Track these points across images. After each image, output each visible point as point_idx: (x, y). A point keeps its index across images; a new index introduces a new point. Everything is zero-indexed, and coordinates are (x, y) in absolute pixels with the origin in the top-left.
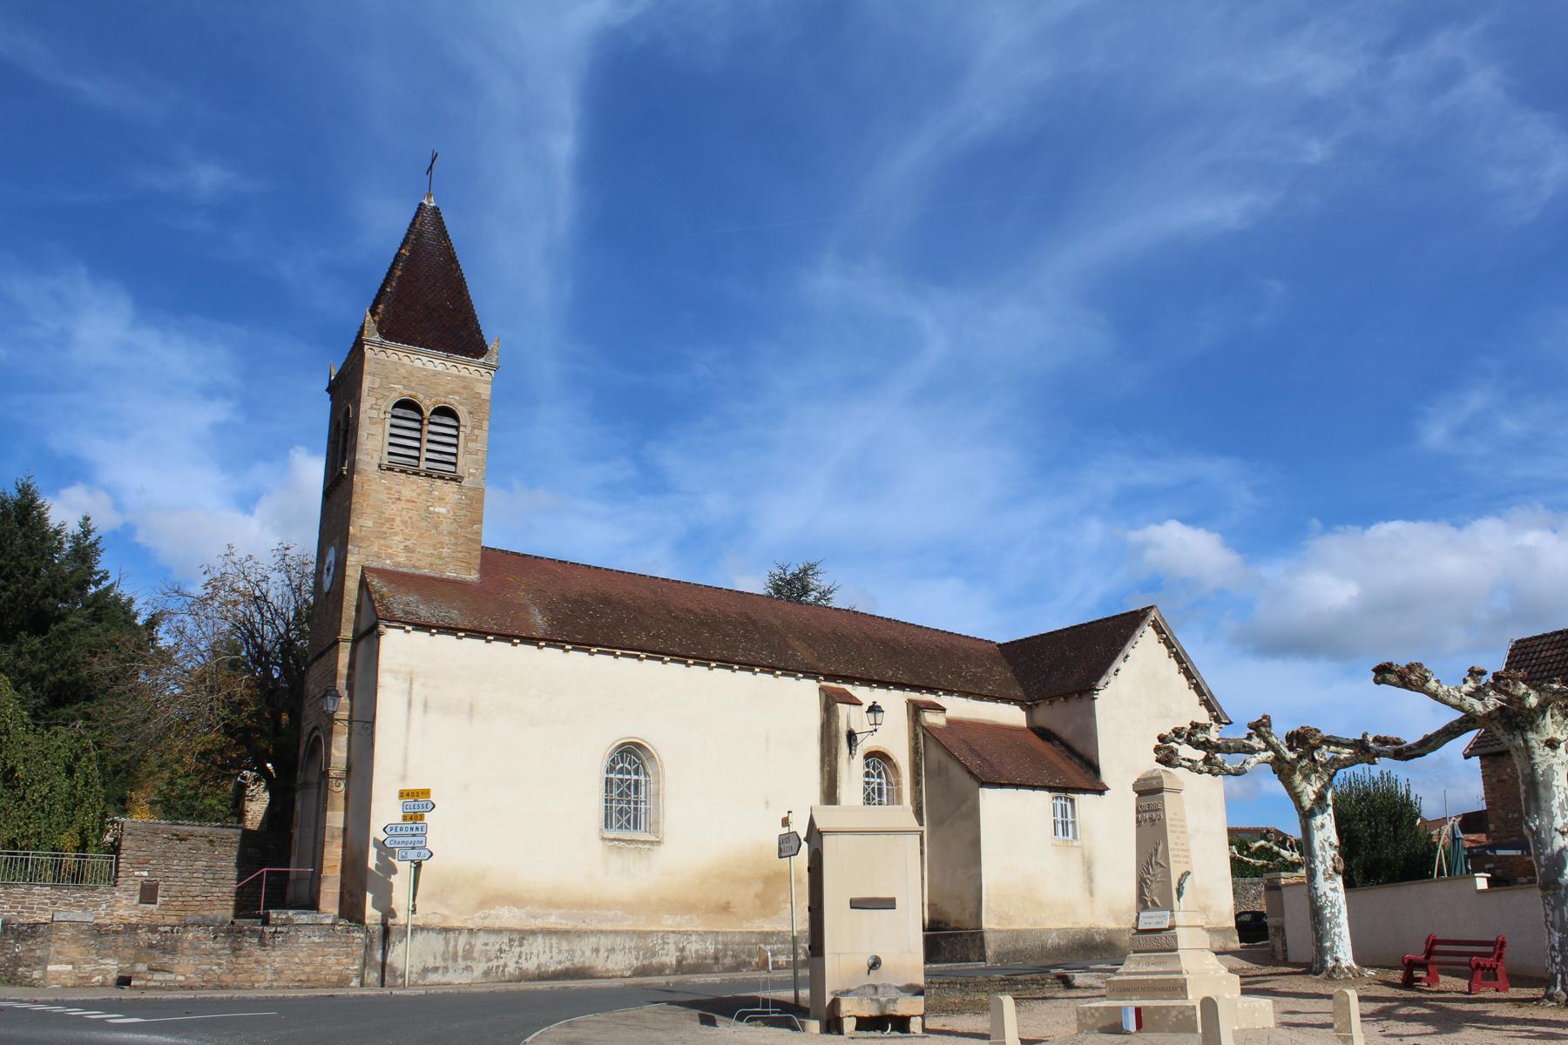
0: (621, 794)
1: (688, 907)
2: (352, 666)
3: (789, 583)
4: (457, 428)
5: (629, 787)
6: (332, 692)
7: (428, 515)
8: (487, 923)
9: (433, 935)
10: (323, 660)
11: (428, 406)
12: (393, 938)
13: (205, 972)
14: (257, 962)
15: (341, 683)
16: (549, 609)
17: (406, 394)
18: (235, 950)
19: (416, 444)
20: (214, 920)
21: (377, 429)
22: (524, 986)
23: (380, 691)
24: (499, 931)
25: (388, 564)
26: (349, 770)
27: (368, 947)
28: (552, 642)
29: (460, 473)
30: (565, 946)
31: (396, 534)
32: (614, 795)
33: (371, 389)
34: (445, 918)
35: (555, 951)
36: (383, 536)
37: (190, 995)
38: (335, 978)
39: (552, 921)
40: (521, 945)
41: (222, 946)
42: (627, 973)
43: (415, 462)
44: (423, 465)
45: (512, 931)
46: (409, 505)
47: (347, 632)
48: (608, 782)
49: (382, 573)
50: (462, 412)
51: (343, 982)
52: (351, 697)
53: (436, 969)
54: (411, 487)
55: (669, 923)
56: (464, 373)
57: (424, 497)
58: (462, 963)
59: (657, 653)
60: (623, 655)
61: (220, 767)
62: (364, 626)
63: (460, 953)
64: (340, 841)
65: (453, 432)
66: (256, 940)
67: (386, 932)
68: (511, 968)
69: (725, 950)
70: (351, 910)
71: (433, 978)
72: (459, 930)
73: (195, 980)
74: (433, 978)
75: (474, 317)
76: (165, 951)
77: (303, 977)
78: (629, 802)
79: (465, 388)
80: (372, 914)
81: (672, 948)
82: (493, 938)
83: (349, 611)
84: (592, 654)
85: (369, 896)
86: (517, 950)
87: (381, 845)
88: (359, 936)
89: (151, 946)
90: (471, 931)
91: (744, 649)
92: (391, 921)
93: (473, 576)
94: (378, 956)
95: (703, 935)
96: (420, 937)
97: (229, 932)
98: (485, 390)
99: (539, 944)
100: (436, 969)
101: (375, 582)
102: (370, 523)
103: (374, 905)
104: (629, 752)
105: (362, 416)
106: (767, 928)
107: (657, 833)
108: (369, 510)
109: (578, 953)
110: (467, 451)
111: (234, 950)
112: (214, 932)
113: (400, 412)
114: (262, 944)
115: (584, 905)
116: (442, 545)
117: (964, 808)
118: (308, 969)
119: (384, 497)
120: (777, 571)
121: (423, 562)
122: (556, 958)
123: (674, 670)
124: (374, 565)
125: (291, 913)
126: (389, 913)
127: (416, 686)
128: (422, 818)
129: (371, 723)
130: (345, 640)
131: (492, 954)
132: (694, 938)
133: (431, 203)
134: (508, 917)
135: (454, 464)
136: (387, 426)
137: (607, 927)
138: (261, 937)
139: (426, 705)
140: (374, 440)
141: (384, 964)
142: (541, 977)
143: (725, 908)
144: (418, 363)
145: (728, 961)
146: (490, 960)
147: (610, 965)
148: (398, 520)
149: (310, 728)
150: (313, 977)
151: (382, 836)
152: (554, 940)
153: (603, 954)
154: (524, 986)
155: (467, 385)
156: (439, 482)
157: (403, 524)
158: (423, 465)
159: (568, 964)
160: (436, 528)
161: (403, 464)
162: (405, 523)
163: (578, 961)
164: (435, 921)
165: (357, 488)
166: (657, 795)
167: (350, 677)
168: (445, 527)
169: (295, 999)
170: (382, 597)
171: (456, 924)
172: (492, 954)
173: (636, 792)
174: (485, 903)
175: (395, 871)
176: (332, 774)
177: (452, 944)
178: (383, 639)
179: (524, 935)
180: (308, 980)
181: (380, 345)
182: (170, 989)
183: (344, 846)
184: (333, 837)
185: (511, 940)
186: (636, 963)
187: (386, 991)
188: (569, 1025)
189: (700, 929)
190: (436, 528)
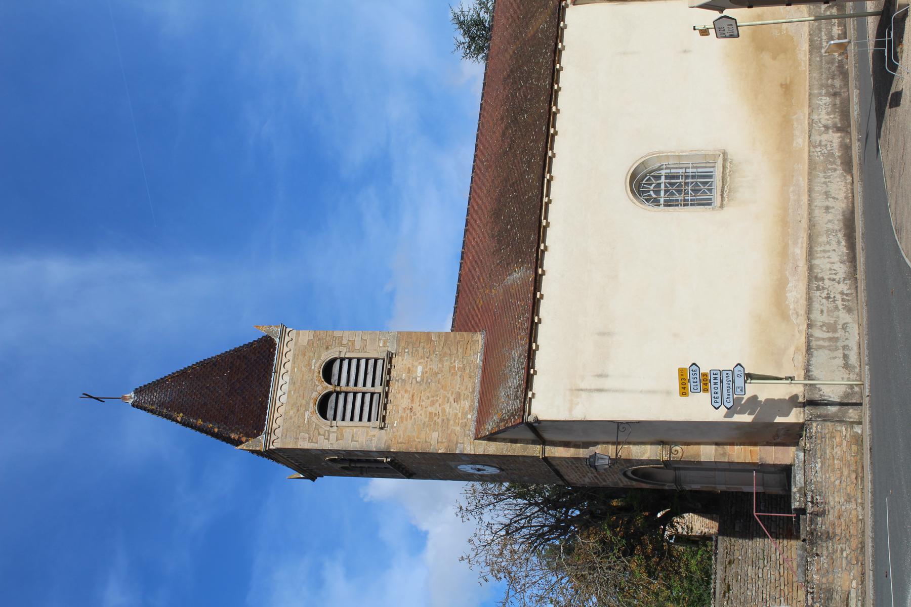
0: (679, 192)
1: (786, 124)
2: (566, 444)
3: (472, 38)
4: (342, 360)
5: (672, 184)
6: (591, 462)
8: (802, 311)
9: (814, 361)
10: (563, 470)
11: (324, 387)
12: (817, 397)
13: (849, 563)
14: (839, 518)
15: (583, 453)
16: (507, 266)
17: (313, 408)
18: (829, 537)
19: (359, 396)
20: (802, 557)
21: (347, 433)
22: (861, 275)
23: (589, 418)
24: (810, 300)
25: (471, 417)
26: (662, 443)
27: (825, 419)
28: (538, 262)
29: (384, 355)
30: (823, 239)
31: (444, 410)
32: (680, 197)
33: (310, 440)
34: (798, 349)
35: (828, 248)
36: (445, 422)
37: (870, 574)
38: (854, 448)
39: (799, 251)
40: (822, 279)
41: (825, 549)
42: (849, 179)
43: (376, 397)
44: (378, 389)
45: (809, 288)
46: (417, 400)
47: (535, 450)
48: (668, 204)
49: (480, 422)
50: (326, 356)
51: (858, 440)
52: (595, 444)
53: (845, 357)
54: (399, 399)
55: (801, 141)
56: (290, 356)
57: (408, 387)
58: (840, 334)
59: (545, 164)
60: (548, 195)
61: (662, 559)
62: (531, 435)
63: (830, 335)
64: (728, 448)
65: (346, 363)
66: (820, 519)
67: (811, 403)
68: (844, 287)
69: (827, 86)
70: (791, 435)
71: (853, 359)
72: (809, 336)
73: (856, 571)
74: (853, 359)
75: (237, 350)
76: (829, 599)
77: (853, 476)
78: (687, 184)
79: (305, 355)
80: (795, 417)
81: (824, 137)
82: (816, 306)
83: (517, 449)
84: (548, 224)
85: (778, 420)
86: (827, 282)
87: (731, 411)
88: (814, 427)
90: (809, 326)
91: (538, 80)
92: (801, 400)
93: (480, 338)
94: (833, 409)
95: (812, 109)
96: (815, 372)
97: (812, 543)
98: (305, 336)
99: (822, 264)
100: (845, 357)
101: (489, 427)
102: (435, 435)
103: (787, 415)
104: (639, 185)
105: (335, 447)
106: (805, 46)
107: (715, 156)
108: (423, 436)
109: (830, 226)
110: (364, 349)
111: (829, 538)
112: (812, 556)
113: (330, 413)
114: (823, 513)
115: (784, 221)
116: (452, 368)
118: (845, 473)
119: (409, 423)
120: (461, 51)
121: (469, 385)
122: (834, 246)
123: (560, 145)
124: (473, 429)
125: (794, 489)
126: (793, 401)
127: (583, 386)
128: (705, 375)
129: (620, 426)
130: (544, 451)
131: (831, 306)
132: (815, 117)
133: (131, 396)
134: (796, 292)
135: (376, 360)
136: (344, 423)
137: (805, 199)
138: (816, 515)
139: (600, 376)
140: (357, 435)
141: (841, 404)
142: (852, 259)
143: (787, 88)
144: (284, 399)
145: (838, 83)
146: (837, 308)
147: (841, 195)
148: (430, 409)
149: (625, 480)
150: (853, 467)
151: (723, 410)
152: (818, 249)
153: (830, 203)
154: (861, 275)
155: (302, 352)
156: (393, 373)
157: (434, 405)
158: (378, 389)
159: (840, 235)
160: (436, 374)
161: (378, 408)
162: (433, 403)
163: (838, 225)
164: (800, 359)
165: (403, 448)
166: (679, 157)
167: (577, 446)
168: (435, 367)
169: (873, 482)
170: (502, 420)
171: (803, 339)
172: (831, 306)
173: (677, 177)
174: (784, 315)
175: (754, 398)
176: (666, 458)
177: (821, 343)
178: (540, 418)
179: (813, 277)
180: (856, 471)
181: (267, 434)
182: (864, 592)
183: (732, 444)
184: (724, 454)
185: (818, 289)
186: (840, 171)
187: (866, 401)
188: (899, 231)
189: (806, 111)
190: (436, 374)
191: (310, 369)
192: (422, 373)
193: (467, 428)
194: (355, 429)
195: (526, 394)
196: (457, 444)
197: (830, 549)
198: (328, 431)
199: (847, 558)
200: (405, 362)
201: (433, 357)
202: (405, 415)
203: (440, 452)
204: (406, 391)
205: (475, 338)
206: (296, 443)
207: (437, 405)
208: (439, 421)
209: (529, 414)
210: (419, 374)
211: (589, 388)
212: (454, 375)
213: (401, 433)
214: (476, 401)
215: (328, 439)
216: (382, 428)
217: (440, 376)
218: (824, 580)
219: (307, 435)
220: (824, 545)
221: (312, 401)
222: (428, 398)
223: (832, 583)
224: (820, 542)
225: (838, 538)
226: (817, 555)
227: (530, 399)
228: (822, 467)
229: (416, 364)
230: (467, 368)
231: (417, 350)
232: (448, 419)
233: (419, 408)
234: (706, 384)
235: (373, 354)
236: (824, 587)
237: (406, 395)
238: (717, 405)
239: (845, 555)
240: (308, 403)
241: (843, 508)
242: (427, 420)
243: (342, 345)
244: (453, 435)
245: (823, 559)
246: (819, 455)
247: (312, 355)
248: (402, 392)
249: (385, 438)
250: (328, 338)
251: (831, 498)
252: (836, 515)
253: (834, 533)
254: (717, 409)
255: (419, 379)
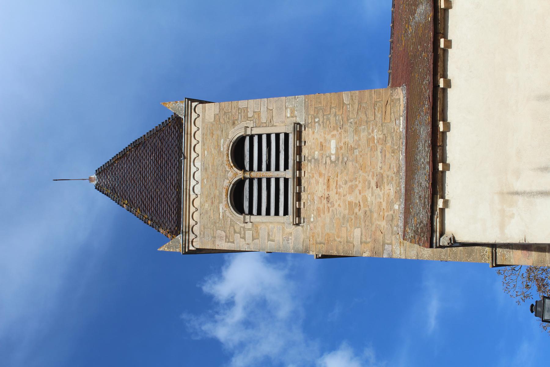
4: (252, 137)
7: (341, 161)
21: (263, 231)
25: (398, 207)
31: (365, 199)
33: (227, 239)
36: (368, 215)
46: (333, 185)
50: (235, 133)
57: (322, 169)
110: (270, 123)
116: (370, 140)
119: (327, 217)
127: (518, 186)
148: (350, 198)
158: (289, 174)
160: (352, 149)
162: (352, 189)
168: (350, 139)
190: (352, 149)
191: (219, 152)
192: (337, 149)
193: (395, 222)
194: (271, 226)
195: (433, 204)
196: (384, 245)
198: (244, 228)
200: (316, 136)
201: (347, 126)
202: (321, 206)
203: (365, 255)
204: (320, 175)
205: (395, 97)
206: (214, 242)
207: (357, 191)
208: (361, 214)
209: (442, 234)
210: (333, 151)
211: (528, 189)
212: (373, 149)
213: (319, 229)
214: (403, 185)
215: (244, 238)
216: (298, 225)
217: (357, 152)
219: (223, 234)
221: (224, 191)
222: (346, 183)
227: (442, 211)
229: (328, 137)
230: (389, 138)
231: (328, 119)
232: (371, 212)
233: (337, 197)
235: (281, 130)
237: (321, 180)
240: (221, 194)
242: (347, 212)
243: (248, 118)
244: (379, 233)
247: (219, 132)
248: (316, 176)
249: (302, 236)
250: (234, 111)
255: (333, 158)
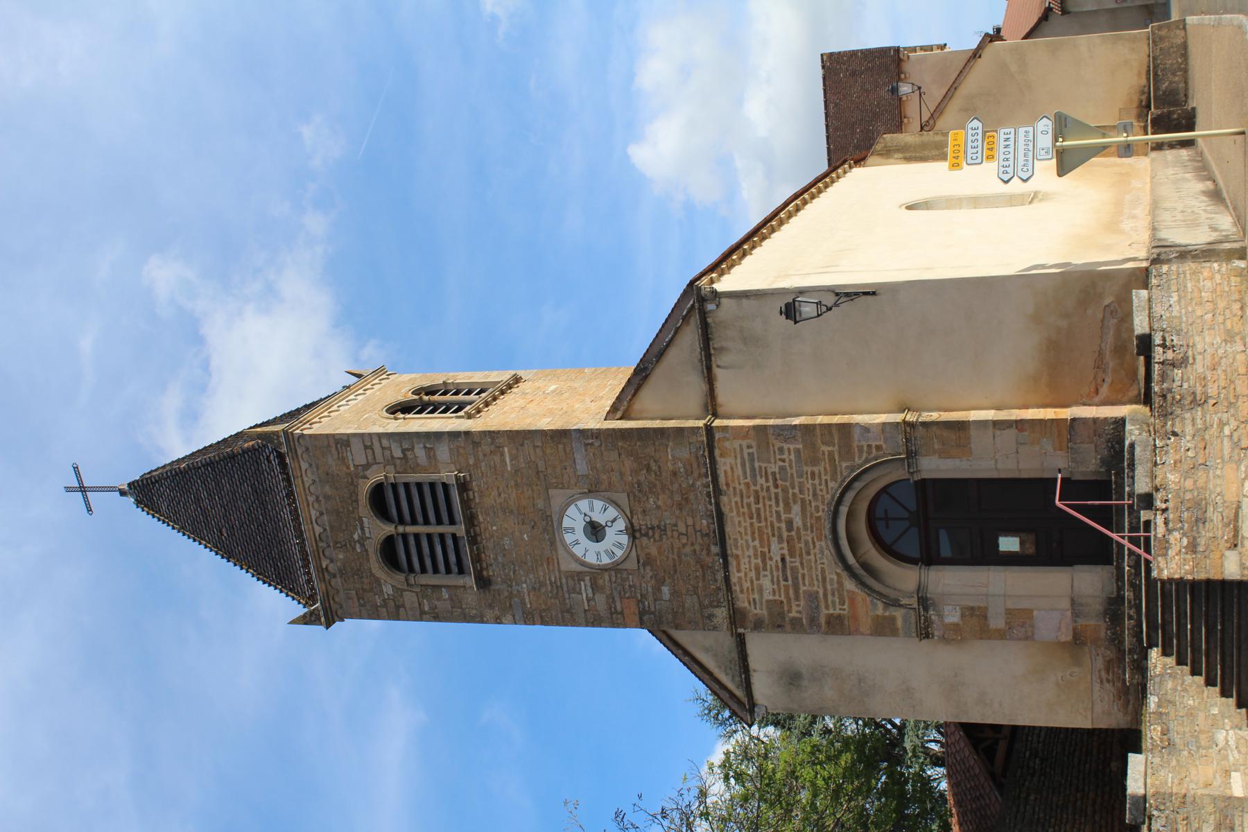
66: (1178, 373)
76: (1201, 520)
89: (1193, 547)
97: (1165, 415)
114: (1183, 362)
117: (1014, 68)
120: (698, 708)
197: (1199, 421)
199: (1231, 436)
218: (1189, 484)
220: (1188, 415)
223: (1205, 488)
224: (1179, 411)
225: (1212, 402)
226: (1175, 434)
228: (1179, 301)
234: (991, 149)
236: (1188, 496)
238: (1006, 177)
239: (1227, 431)
241: (1221, 352)
245: (1186, 442)
246: (1174, 288)
251: (1197, 339)
252: (1208, 361)
253: (1205, 393)
254: (1006, 182)
